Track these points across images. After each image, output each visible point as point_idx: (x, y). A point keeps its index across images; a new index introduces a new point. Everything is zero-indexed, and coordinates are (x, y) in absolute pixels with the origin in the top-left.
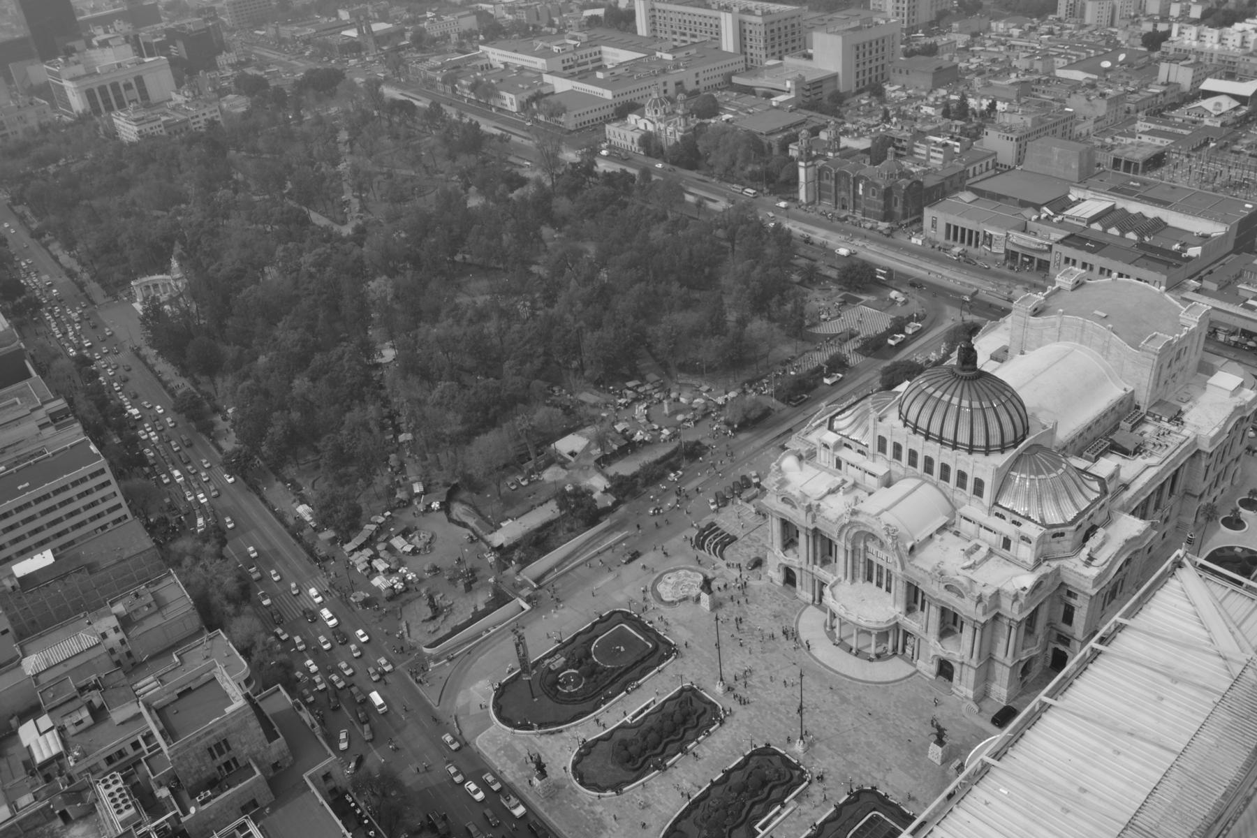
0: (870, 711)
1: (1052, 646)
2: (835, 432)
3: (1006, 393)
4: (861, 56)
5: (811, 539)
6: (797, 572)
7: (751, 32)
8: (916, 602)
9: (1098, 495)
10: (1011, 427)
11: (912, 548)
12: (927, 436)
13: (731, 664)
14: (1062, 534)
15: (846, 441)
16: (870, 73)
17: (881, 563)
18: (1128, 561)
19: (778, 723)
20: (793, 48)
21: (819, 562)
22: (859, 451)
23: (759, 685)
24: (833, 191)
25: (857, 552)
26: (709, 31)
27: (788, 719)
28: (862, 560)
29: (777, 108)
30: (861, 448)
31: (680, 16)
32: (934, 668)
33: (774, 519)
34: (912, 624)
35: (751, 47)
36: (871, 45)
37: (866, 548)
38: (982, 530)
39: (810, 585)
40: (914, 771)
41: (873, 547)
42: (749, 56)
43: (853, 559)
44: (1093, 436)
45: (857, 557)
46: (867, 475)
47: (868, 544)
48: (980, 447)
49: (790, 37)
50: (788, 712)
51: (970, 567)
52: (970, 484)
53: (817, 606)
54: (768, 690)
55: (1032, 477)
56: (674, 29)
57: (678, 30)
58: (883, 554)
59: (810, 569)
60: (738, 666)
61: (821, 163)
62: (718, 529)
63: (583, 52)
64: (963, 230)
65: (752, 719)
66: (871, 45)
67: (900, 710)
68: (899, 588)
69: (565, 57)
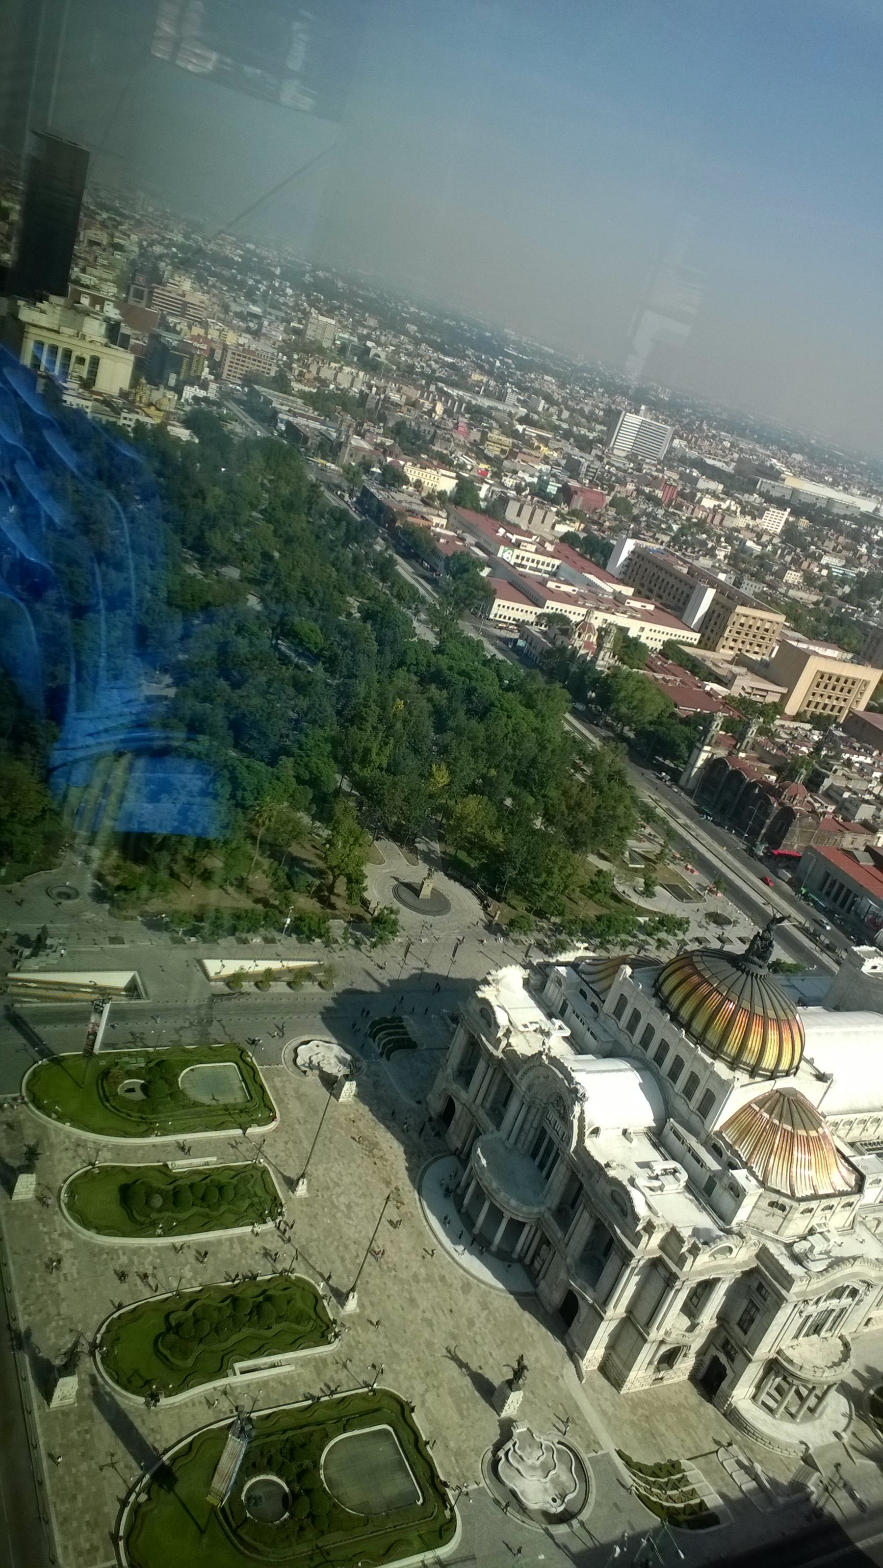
0: (454, 1308)
1: (713, 1352)
2: (578, 973)
3: (788, 1011)
4: (822, 685)
5: (491, 1071)
6: (458, 1107)
7: (719, 615)
8: (573, 1205)
9: (847, 1188)
10: (776, 1052)
11: (596, 1131)
12: (675, 1018)
13: (326, 1169)
14: (783, 1208)
15: (586, 988)
16: (824, 708)
17: (554, 1138)
18: (854, 1293)
19: (338, 1263)
20: (756, 653)
21: (488, 1105)
22: (593, 1005)
23: (343, 1208)
24: (720, 788)
25: (533, 1111)
26: (677, 597)
27: (353, 1263)
28: (535, 1125)
29: (708, 693)
30: (596, 1002)
31: (655, 570)
32: (557, 1298)
33: (462, 1031)
34: (555, 1232)
35: (712, 631)
36: (838, 680)
37: (545, 1111)
38: (689, 1155)
39: (465, 1129)
40: (465, 1406)
41: (553, 1116)
42: (706, 637)
43: (525, 1119)
44: (877, 1134)
45: (531, 1117)
46: (588, 1034)
47: (550, 1108)
48: (729, 1056)
49: (758, 640)
50: (357, 1256)
51: (651, 1189)
52: (698, 1095)
53: (460, 1160)
54: (350, 1218)
55: (776, 1122)
56: (644, 581)
57: (646, 584)
58: (560, 1126)
59: (473, 1108)
60: (333, 1175)
61: (721, 753)
62: (403, 1027)
63: (542, 558)
64: (842, 886)
65: (312, 1240)
66: (838, 680)
67: (490, 1326)
68: (559, 1175)
69: (522, 554)
